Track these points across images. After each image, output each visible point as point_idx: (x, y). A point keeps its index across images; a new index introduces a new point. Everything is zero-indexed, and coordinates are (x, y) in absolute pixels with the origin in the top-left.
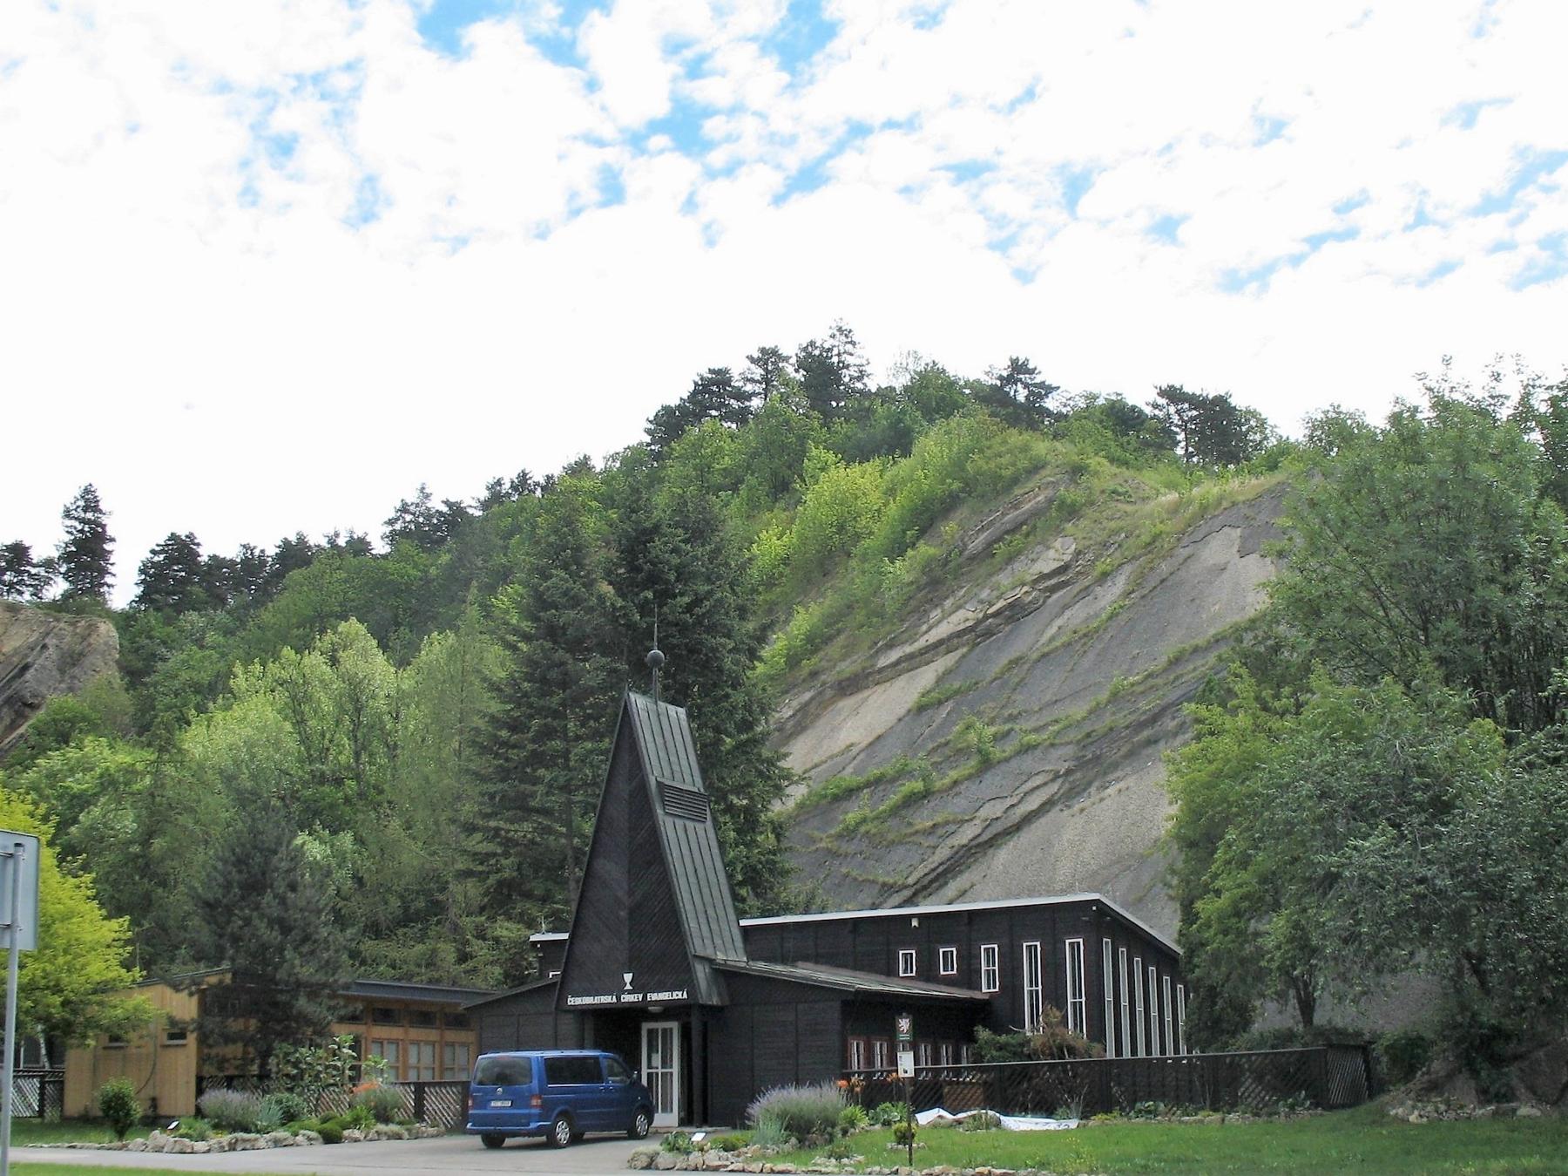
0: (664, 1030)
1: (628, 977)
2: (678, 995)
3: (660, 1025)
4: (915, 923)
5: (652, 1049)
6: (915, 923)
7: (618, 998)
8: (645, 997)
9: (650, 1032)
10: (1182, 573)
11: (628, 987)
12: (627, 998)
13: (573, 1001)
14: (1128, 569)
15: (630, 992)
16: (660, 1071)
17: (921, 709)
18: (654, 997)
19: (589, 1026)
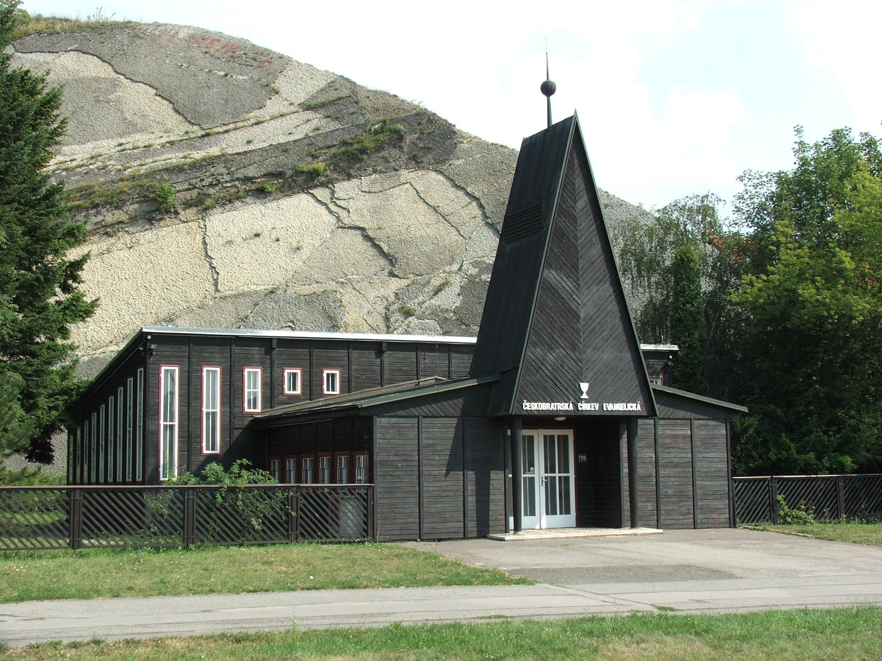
2: (634, 407)
7: (576, 406)
8: (601, 407)
11: (585, 396)
12: (585, 407)
15: (587, 401)
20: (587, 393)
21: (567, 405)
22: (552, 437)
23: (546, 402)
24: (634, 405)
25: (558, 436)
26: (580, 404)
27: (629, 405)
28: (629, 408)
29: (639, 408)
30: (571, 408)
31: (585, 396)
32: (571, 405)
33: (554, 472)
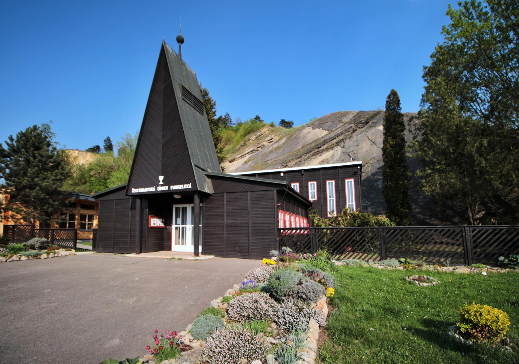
0: (183, 208)
1: (161, 178)
2: (188, 186)
4: (282, 174)
5: (177, 216)
6: (282, 174)
7: (156, 189)
8: (169, 188)
10: (299, 135)
11: (161, 183)
12: (160, 189)
13: (135, 191)
15: (162, 185)
17: (245, 163)
18: (174, 188)
19: (146, 203)
23: (142, 188)
24: (187, 185)
27: (185, 185)
28: (185, 187)
29: (190, 187)
30: (154, 190)
31: (161, 183)
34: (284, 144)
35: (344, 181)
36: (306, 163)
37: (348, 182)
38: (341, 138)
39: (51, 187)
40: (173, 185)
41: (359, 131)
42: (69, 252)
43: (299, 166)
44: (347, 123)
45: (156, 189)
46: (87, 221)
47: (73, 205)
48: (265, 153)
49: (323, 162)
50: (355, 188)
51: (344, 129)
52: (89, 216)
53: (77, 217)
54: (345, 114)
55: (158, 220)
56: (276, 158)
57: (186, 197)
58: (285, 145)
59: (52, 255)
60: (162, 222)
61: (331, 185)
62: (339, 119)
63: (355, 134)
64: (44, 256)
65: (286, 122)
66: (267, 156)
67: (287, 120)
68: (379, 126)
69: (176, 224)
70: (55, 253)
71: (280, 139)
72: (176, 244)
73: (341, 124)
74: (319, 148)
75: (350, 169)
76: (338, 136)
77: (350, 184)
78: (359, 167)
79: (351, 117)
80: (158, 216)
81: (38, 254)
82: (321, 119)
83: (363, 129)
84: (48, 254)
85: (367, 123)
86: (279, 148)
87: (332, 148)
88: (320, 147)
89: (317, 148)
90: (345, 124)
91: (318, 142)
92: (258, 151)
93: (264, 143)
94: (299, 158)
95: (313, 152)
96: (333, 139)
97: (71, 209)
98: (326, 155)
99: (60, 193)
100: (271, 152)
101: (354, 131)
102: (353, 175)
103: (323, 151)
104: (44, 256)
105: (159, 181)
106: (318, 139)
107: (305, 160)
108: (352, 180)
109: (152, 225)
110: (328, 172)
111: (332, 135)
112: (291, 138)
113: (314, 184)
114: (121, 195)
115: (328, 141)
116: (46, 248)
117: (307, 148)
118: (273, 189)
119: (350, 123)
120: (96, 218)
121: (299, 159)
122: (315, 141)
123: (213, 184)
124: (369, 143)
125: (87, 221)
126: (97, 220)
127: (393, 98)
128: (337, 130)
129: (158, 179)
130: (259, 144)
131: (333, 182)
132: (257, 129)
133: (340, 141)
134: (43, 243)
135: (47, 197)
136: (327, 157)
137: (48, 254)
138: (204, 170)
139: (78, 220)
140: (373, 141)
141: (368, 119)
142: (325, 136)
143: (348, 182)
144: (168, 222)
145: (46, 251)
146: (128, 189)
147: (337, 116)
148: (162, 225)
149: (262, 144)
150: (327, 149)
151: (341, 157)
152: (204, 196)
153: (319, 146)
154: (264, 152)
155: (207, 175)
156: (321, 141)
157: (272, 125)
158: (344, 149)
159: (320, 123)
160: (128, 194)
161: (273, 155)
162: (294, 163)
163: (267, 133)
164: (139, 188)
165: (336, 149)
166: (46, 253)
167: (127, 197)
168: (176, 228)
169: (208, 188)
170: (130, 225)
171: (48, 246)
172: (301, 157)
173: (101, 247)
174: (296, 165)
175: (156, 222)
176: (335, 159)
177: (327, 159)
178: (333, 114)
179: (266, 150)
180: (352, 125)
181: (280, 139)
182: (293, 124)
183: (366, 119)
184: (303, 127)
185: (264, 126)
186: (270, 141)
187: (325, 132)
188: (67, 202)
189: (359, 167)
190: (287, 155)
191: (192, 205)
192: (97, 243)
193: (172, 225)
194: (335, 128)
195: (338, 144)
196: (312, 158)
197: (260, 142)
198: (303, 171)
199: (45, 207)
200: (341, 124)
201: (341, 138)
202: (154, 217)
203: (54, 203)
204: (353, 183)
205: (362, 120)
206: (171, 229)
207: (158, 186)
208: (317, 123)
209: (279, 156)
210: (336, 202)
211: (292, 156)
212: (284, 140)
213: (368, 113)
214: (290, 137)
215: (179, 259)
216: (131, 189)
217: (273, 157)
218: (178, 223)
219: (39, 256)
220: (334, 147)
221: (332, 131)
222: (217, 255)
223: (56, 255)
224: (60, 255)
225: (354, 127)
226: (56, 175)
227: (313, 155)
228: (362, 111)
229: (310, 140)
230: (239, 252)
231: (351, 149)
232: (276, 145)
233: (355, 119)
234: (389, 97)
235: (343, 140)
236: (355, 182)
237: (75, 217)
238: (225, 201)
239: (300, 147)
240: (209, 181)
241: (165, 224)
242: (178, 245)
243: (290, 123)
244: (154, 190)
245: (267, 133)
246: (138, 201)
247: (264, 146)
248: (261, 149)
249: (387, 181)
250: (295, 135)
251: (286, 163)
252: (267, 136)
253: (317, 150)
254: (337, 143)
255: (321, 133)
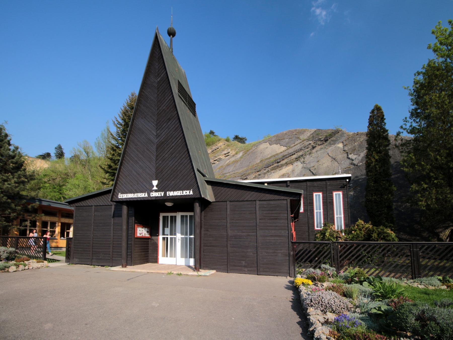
0: (172, 217)
1: (155, 183)
2: (188, 193)
3: (169, 215)
4: (266, 184)
7: (149, 194)
8: (165, 194)
9: (164, 218)
11: (155, 188)
12: (154, 194)
13: (122, 196)
14: (242, 152)
15: (156, 191)
16: (169, 237)
20: (157, 186)
21: (144, 194)
22: (187, 216)
23: (131, 193)
25: (190, 216)
26: (151, 193)
28: (184, 194)
29: (191, 193)
30: (146, 195)
32: (146, 194)
33: (187, 235)
34: (241, 158)
35: (332, 193)
36: (266, 177)
37: (316, 195)
38: (300, 154)
39: (12, 190)
40: (171, 191)
41: (318, 148)
42: (41, 263)
43: (258, 179)
44: (305, 140)
45: (149, 194)
46: (49, 228)
47: (35, 211)
48: (222, 166)
49: (283, 176)
50: (343, 201)
51: (303, 146)
52: (51, 223)
53: (37, 223)
54: (302, 132)
55: (143, 229)
56: (234, 171)
57: (183, 205)
58: (242, 159)
59: (21, 267)
60: (148, 232)
61: (318, 198)
62: (296, 136)
63: (314, 151)
64: (13, 268)
65: (239, 138)
66: (224, 169)
67: (240, 136)
68: (338, 143)
69: (164, 234)
70: (25, 265)
71: (236, 154)
72: (163, 256)
73: (299, 141)
74: (278, 162)
75: (339, 182)
76: (297, 152)
77: (338, 197)
78: (348, 180)
79: (309, 135)
80: (144, 225)
81: (5, 267)
82: (277, 136)
83: (322, 146)
84: (18, 266)
85: (326, 140)
86: (236, 162)
87: (291, 163)
88: (280, 162)
89: (276, 163)
90: (303, 141)
91: (277, 157)
92: (214, 163)
93: (221, 157)
94: (258, 172)
95: (272, 166)
96: (293, 155)
97: (33, 215)
98: (285, 170)
99: (21, 197)
100: (228, 165)
101: (314, 148)
102: (341, 187)
103: (282, 166)
104: (13, 268)
105: (153, 186)
106: (277, 154)
107: (264, 174)
108: (341, 193)
109: (138, 235)
110: (315, 184)
111: (291, 151)
112: (248, 153)
113: (339, 194)
114: (106, 200)
115: (287, 156)
116: (13, 259)
117: (266, 162)
118: (286, 198)
119: (308, 140)
120: (59, 226)
121: (259, 173)
122: (274, 156)
123: (213, 191)
124: (330, 159)
125: (49, 228)
126: (60, 227)
127: (377, 113)
128: (296, 146)
129: (152, 184)
130: (216, 157)
131: (321, 194)
132: (213, 143)
133: (299, 157)
134: (10, 253)
135: (9, 200)
136: (288, 172)
137: (18, 266)
138: (204, 176)
139: (39, 226)
140: (334, 157)
141: (326, 137)
142: (283, 151)
143: (316, 195)
144: (154, 231)
145: (13, 262)
146: (113, 194)
147: (294, 133)
148: (147, 235)
149: (218, 157)
150: (287, 164)
151: (301, 172)
152: (205, 203)
153: (278, 161)
154: (221, 165)
155: (206, 181)
156: (280, 156)
157: (227, 140)
158: (305, 165)
159: (278, 140)
160: (114, 200)
161: (231, 169)
162: (254, 176)
163: (223, 147)
164: (127, 193)
165: (296, 164)
166: (15, 265)
167: (112, 203)
168: (164, 239)
169: (208, 194)
170: (112, 235)
171: (15, 256)
172: (260, 171)
173: (76, 258)
174: (255, 178)
175: (142, 232)
176: (296, 174)
177: (288, 174)
178: (290, 131)
179: (222, 163)
180: (311, 142)
181: (236, 154)
182: (246, 140)
183: (324, 136)
184: (260, 143)
185: (220, 140)
186: (227, 155)
187: (283, 148)
188: (30, 207)
189: (348, 180)
190: (245, 168)
191: (192, 214)
192: (72, 254)
193: (158, 236)
194: (294, 145)
195: (297, 159)
196: (272, 172)
197: (216, 155)
198: (288, 182)
199: (7, 212)
200: (299, 141)
201: (300, 154)
202: (138, 226)
203: (17, 208)
204: (341, 196)
205: (321, 137)
206: (158, 240)
207: (152, 191)
208: (273, 139)
209: (237, 170)
210: (324, 215)
211: (251, 169)
212: (241, 154)
213: (325, 131)
214: (246, 152)
215: (178, 274)
216: (118, 195)
217: (231, 170)
218: (166, 233)
219: (7, 269)
220: (294, 162)
221: (290, 148)
222: (218, 270)
223: (27, 267)
224: (31, 268)
225: (313, 144)
226: (19, 177)
227: (273, 169)
228: (319, 130)
229: (268, 155)
230: (245, 267)
231: (312, 165)
232: (233, 159)
233: (313, 137)
234: (373, 112)
235: (302, 155)
236: (343, 195)
237: (36, 224)
238: (228, 210)
239: (259, 161)
240: (209, 187)
241: (151, 234)
242: (165, 258)
243: (244, 139)
244: (146, 195)
245: (223, 147)
246: (125, 208)
247: (220, 159)
248: (217, 163)
249: (372, 194)
250: (251, 150)
251: (245, 176)
252: (223, 150)
253: (276, 165)
254: (296, 158)
255: (279, 149)
